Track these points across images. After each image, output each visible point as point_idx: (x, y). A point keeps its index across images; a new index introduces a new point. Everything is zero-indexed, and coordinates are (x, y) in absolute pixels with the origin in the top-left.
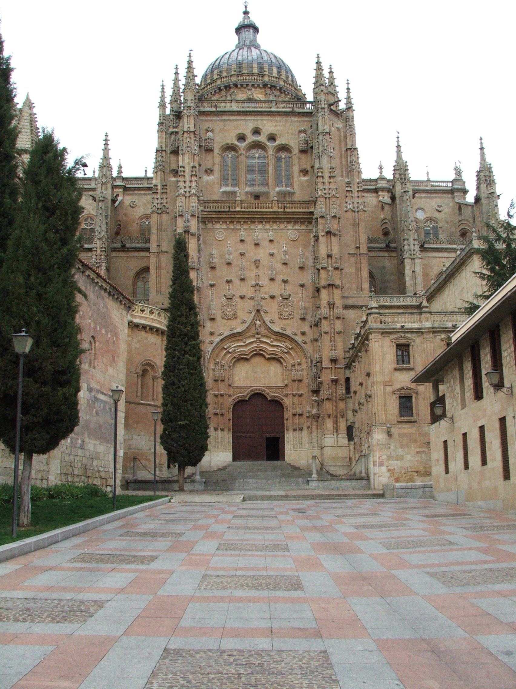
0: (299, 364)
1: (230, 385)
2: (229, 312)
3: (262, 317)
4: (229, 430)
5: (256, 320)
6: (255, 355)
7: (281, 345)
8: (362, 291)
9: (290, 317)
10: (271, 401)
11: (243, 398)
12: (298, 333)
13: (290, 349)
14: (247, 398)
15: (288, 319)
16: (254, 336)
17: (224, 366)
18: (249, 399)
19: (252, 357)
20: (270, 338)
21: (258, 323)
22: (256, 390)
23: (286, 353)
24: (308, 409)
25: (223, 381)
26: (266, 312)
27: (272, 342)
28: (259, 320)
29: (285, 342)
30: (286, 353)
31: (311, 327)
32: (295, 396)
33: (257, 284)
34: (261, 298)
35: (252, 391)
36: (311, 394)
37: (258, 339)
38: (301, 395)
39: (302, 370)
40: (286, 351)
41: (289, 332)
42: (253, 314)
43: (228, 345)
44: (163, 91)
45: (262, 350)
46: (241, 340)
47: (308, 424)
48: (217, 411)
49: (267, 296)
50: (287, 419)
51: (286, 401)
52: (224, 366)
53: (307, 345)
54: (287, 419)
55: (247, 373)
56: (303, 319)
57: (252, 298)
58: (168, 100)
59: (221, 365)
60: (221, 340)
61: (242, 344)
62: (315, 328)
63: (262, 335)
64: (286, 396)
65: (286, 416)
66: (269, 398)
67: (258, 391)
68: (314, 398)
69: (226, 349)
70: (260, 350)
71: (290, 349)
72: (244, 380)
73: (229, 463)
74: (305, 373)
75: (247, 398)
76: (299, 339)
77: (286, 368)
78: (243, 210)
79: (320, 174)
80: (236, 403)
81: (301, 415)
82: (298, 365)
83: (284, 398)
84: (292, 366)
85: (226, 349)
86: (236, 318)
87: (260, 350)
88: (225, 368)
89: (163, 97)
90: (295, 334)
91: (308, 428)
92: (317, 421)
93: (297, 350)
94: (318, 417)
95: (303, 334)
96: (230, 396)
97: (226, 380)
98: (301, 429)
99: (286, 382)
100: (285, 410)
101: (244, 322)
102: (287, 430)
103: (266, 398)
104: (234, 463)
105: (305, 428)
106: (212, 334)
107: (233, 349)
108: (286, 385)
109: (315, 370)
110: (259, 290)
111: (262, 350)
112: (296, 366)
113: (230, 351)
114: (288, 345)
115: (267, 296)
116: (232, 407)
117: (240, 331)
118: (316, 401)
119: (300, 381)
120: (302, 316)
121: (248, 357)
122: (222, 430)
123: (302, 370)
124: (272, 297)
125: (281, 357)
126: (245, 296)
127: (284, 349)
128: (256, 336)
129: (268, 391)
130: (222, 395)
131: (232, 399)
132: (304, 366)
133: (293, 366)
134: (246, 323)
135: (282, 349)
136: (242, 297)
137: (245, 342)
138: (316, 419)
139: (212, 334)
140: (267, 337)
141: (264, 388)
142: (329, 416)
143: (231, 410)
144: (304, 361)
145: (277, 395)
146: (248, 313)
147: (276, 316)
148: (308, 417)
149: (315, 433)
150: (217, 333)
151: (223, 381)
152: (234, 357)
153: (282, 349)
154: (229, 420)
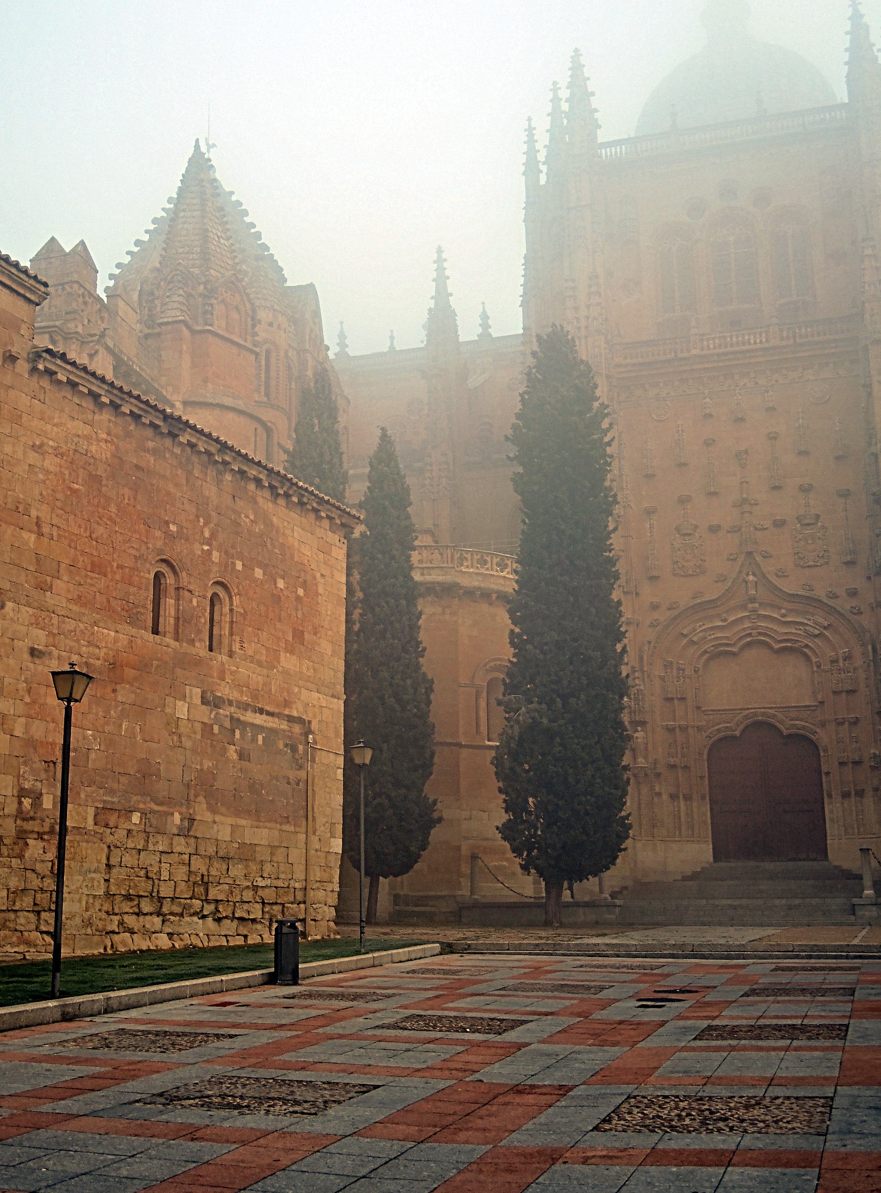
0: (848, 657)
1: (698, 708)
2: (687, 561)
3: (758, 565)
5: (748, 575)
6: (749, 645)
7: (806, 621)
9: (821, 561)
10: (790, 736)
11: (729, 733)
13: (825, 628)
14: (737, 733)
16: (744, 607)
17: (683, 670)
19: (742, 649)
20: (780, 608)
21: (751, 578)
22: (755, 714)
23: (816, 636)
25: (683, 699)
26: (766, 556)
27: (783, 616)
28: (754, 575)
29: (813, 615)
30: (816, 636)
31: (869, 578)
32: (842, 723)
33: (745, 501)
34: (756, 529)
35: (746, 717)
37: (754, 610)
38: (856, 722)
39: (855, 669)
40: (817, 632)
41: (820, 593)
42: (740, 561)
43: (690, 628)
44: (531, 141)
46: (718, 615)
49: (767, 523)
51: (823, 737)
52: (683, 670)
54: (828, 773)
56: (850, 563)
57: (736, 530)
58: (541, 156)
59: (679, 669)
60: (675, 618)
61: (721, 624)
63: (761, 604)
66: (785, 732)
69: (686, 636)
70: (760, 634)
71: (825, 628)
75: (737, 733)
77: (819, 667)
79: (868, 252)
82: (845, 660)
83: (818, 730)
84: (832, 662)
85: (686, 636)
86: (703, 572)
87: (760, 634)
88: (687, 672)
89: (531, 153)
90: (835, 596)
96: (699, 729)
98: (860, 794)
99: (820, 698)
101: (722, 579)
102: (830, 796)
104: (716, 865)
105: (869, 793)
106: (655, 607)
107: (701, 635)
108: (822, 703)
110: (750, 513)
111: (765, 635)
113: (695, 639)
114: (821, 620)
115: (767, 523)
116: (706, 752)
117: (714, 598)
119: (850, 692)
120: (848, 558)
121: (735, 649)
123: (855, 669)
124: (780, 524)
125: (807, 646)
126: (719, 526)
127: (811, 630)
128: (750, 606)
129: (780, 716)
130: (683, 729)
131: (705, 735)
133: (834, 661)
134: (725, 580)
135: (807, 628)
136: (714, 529)
137: (725, 620)
140: (773, 606)
143: (705, 757)
145: (803, 723)
146: (728, 559)
152: (705, 652)
153: (807, 628)
154: (702, 778)
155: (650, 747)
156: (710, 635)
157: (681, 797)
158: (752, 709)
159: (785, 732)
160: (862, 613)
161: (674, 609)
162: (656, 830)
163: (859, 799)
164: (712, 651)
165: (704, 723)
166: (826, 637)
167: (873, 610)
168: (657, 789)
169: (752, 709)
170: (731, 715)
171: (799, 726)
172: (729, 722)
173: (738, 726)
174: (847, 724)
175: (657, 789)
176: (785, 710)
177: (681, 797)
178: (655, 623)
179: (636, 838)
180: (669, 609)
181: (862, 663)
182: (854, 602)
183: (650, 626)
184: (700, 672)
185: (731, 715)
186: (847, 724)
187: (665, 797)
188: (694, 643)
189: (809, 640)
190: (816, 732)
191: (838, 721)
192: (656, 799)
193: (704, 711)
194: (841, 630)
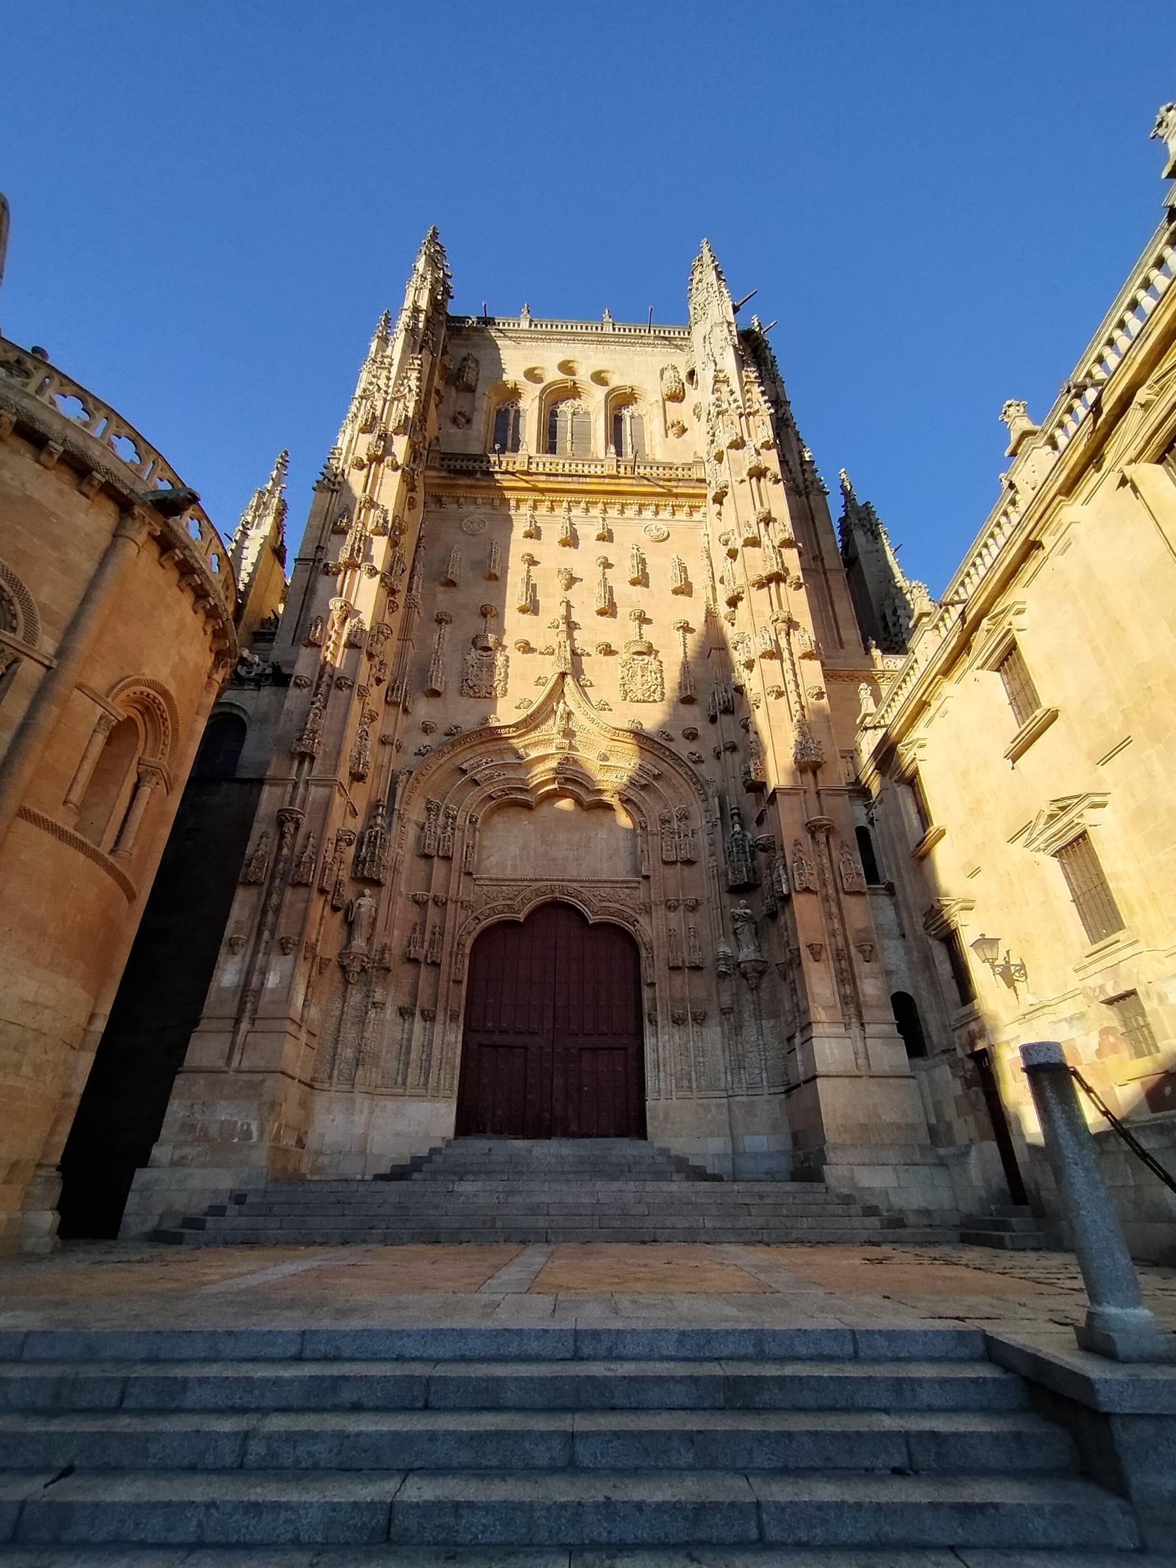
0: (684, 817)
1: (470, 874)
4: (454, 1017)
8: (842, 647)
11: (509, 916)
12: (677, 734)
14: (521, 917)
15: (644, 701)
18: (529, 917)
23: (644, 787)
24: (724, 949)
25: (448, 859)
32: (675, 908)
35: (538, 893)
36: (727, 899)
40: (644, 782)
45: (575, 782)
47: (726, 999)
48: (419, 952)
50: (652, 985)
51: (649, 929)
52: (454, 818)
53: (703, 766)
55: (524, 847)
62: (724, 719)
64: (647, 910)
65: (647, 974)
66: (592, 919)
67: (557, 895)
68: (739, 911)
70: (567, 779)
72: (515, 867)
73: (439, 1144)
74: (703, 839)
75: (521, 917)
76: (683, 748)
78: (534, 470)
80: (486, 932)
81: (697, 968)
83: (639, 918)
85: (464, 772)
91: (724, 1012)
92: (757, 987)
93: (677, 780)
94: (762, 974)
95: (692, 736)
96: (465, 905)
97: (456, 856)
100: (644, 953)
103: (584, 919)
109: (737, 828)
111: (575, 782)
112: (675, 825)
116: (469, 943)
118: (747, 919)
119: (689, 862)
122: (429, 1017)
129: (587, 894)
130: (438, 903)
132: (698, 821)
138: (753, 982)
139: (426, 729)
141: (575, 885)
142: (816, 952)
143: (468, 951)
144: (697, 810)
147: (613, 695)
148: (722, 976)
149: (750, 1032)
150: (443, 727)
151: (448, 859)
155: (380, 924)
156: (499, 775)
157: (418, 1013)
158: (547, 880)
159: (592, 919)
160: (702, 762)
161: (453, 735)
162: (360, 1072)
163: (697, 1028)
164: (500, 797)
165: (472, 898)
166: (656, 790)
167: (718, 758)
168: (378, 997)
169: (547, 880)
170: (515, 888)
171: (612, 910)
172: (510, 899)
173: (524, 904)
174: (682, 908)
175: (378, 997)
176: (593, 885)
177: (418, 1013)
178: (424, 751)
179: (317, 1085)
180: (447, 735)
181: (704, 823)
182: (693, 747)
183: (416, 754)
184: (478, 825)
185: (515, 888)
186: (682, 908)
187: (390, 1013)
188: (476, 783)
189: (632, 793)
190: (636, 920)
191: (669, 903)
192: (372, 1014)
193: (475, 880)
194: (674, 781)
